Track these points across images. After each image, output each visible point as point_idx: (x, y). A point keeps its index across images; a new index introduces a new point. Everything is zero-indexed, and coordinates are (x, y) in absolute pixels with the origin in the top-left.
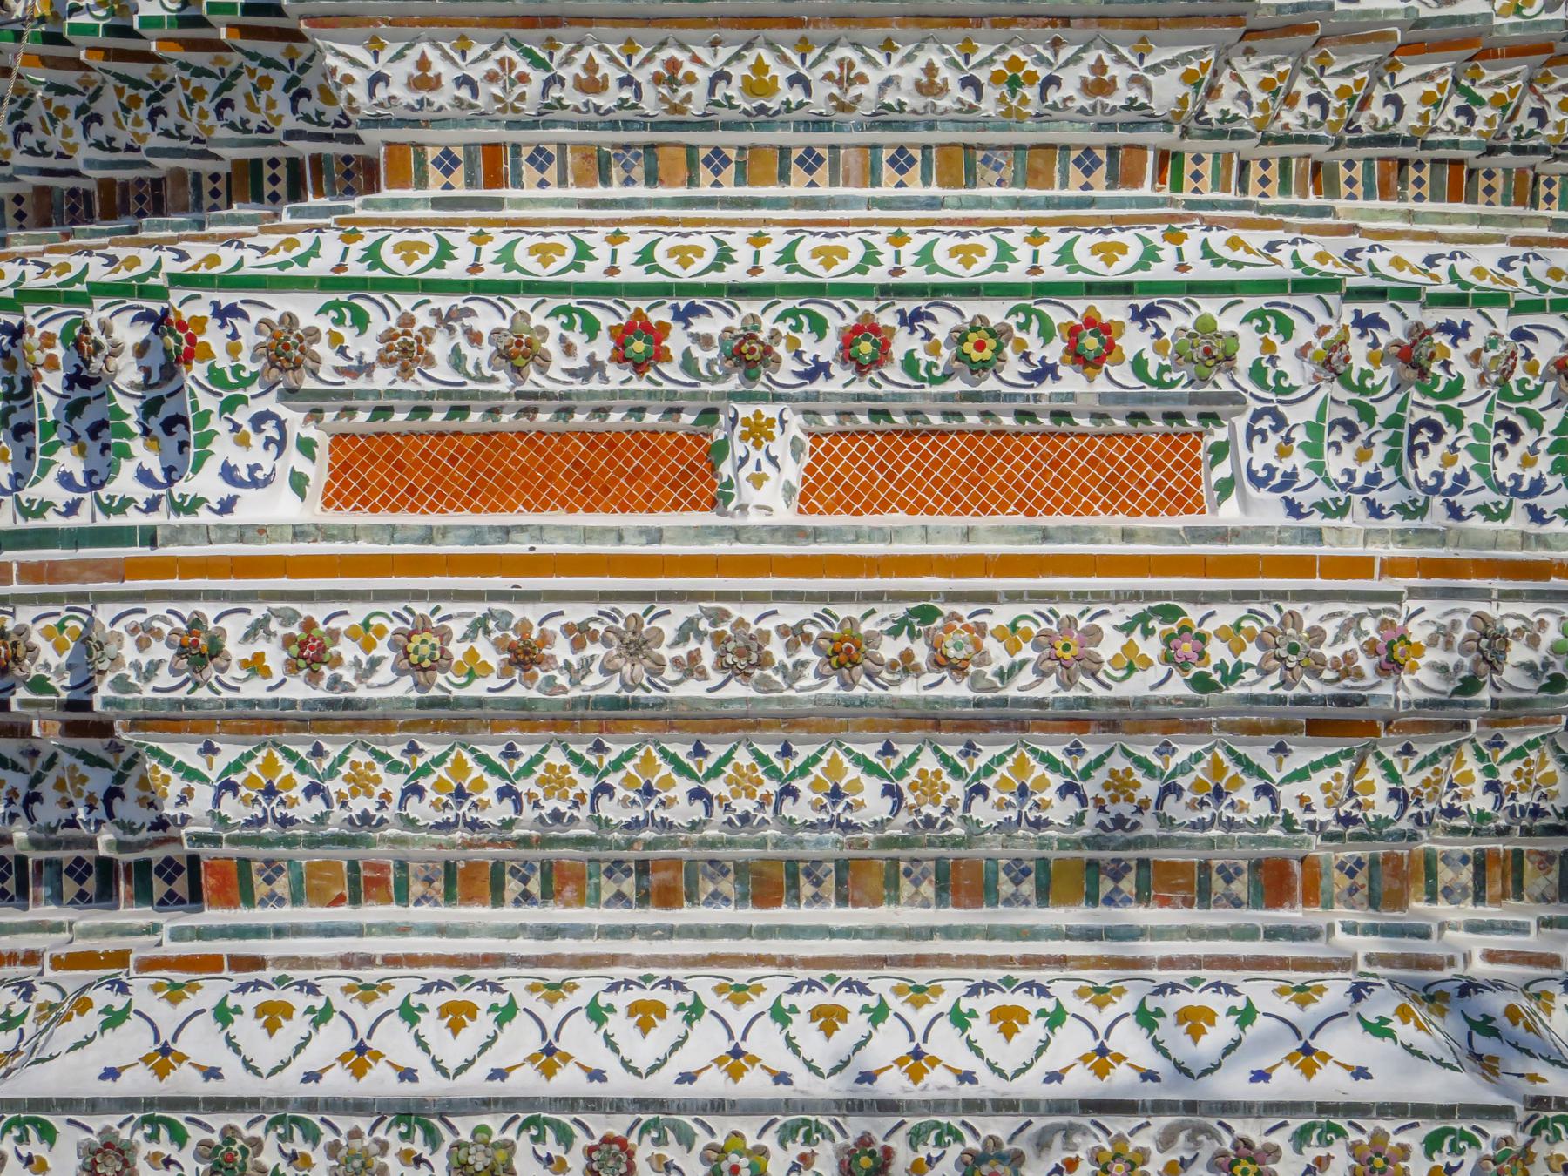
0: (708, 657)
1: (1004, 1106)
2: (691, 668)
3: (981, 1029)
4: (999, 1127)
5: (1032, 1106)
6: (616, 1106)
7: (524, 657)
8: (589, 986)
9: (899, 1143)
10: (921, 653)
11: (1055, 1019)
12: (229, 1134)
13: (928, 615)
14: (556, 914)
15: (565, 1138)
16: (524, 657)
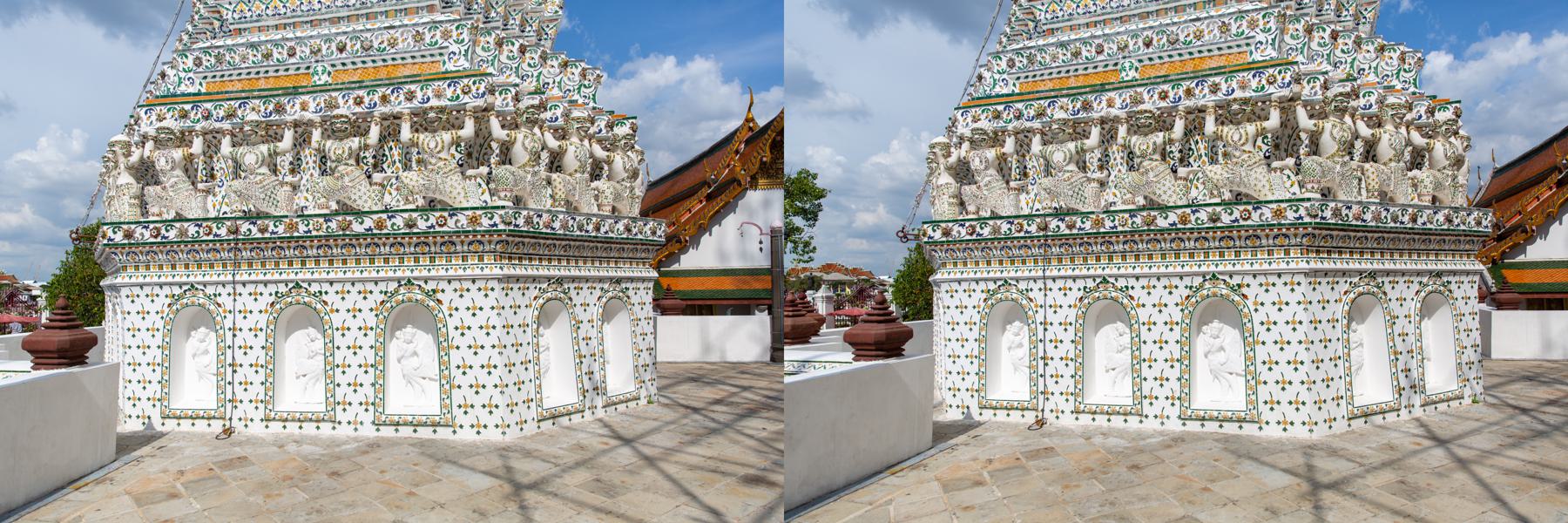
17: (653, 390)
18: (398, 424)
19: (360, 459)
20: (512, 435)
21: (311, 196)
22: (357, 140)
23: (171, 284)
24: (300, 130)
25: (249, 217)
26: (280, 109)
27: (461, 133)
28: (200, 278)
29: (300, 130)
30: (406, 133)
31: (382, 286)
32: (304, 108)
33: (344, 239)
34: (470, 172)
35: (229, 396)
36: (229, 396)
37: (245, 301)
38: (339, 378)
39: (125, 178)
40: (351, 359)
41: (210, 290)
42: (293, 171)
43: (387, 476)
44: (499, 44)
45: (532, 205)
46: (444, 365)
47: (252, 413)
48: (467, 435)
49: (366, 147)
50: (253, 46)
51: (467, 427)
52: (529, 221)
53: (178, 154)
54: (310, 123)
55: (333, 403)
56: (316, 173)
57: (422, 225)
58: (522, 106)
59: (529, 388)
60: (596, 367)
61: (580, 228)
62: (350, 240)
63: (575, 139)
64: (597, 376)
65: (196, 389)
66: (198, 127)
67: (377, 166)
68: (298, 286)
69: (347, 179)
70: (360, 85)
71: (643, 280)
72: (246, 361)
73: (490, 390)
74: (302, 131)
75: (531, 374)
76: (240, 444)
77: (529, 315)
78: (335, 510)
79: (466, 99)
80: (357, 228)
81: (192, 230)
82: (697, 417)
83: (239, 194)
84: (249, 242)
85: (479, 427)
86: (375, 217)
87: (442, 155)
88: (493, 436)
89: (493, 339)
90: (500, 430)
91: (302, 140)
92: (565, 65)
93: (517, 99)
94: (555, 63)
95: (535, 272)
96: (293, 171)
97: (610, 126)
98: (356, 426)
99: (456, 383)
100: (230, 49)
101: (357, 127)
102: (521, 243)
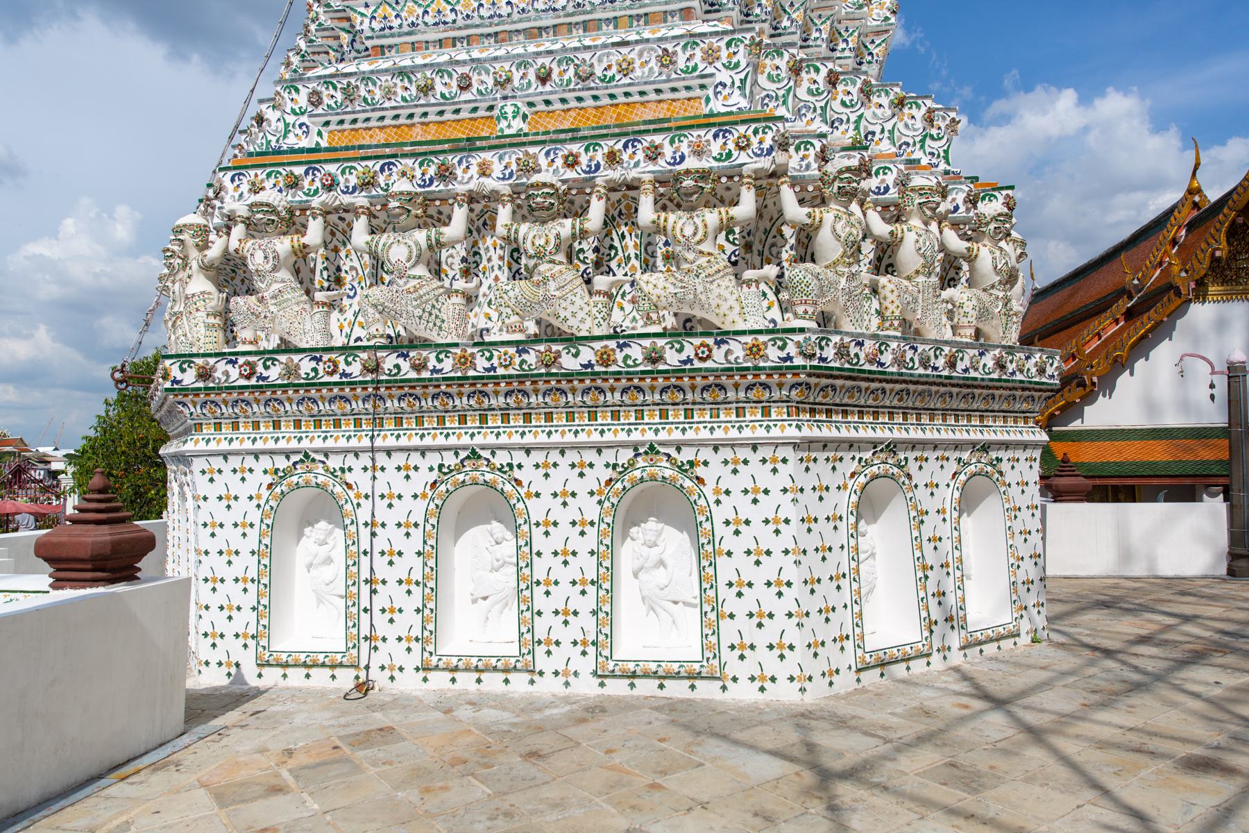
9: (554, 66)
12: (349, 84)
15: (450, 76)
17: (1041, 621)
18: (634, 675)
19: (573, 732)
20: (817, 693)
21: (496, 312)
22: (568, 222)
23: (271, 453)
24: (478, 207)
25: (396, 345)
26: (445, 174)
27: (735, 211)
28: (318, 443)
29: (478, 207)
30: (647, 212)
31: (609, 456)
32: (484, 171)
33: (548, 380)
34: (749, 274)
35: (365, 631)
36: (365, 631)
37: (391, 479)
38: (540, 602)
39: (200, 284)
40: (559, 572)
41: (335, 462)
42: (466, 273)
43: (617, 759)
44: (796, 70)
45: (847, 326)
46: (707, 581)
47: (401, 657)
48: (744, 693)
49: (584, 234)
50: (403, 73)
51: (744, 680)
52: (842, 351)
53: (283, 245)
54: (494, 196)
55: (530, 641)
56: (504, 276)
57: (672, 358)
58: (831, 168)
59: (844, 618)
60: (949, 585)
61: (925, 363)
62: (558, 383)
63: (915, 222)
64: (951, 599)
65: (312, 620)
66: (316, 202)
67: (601, 265)
68: (474, 455)
69: (552, 285)
70: (574, 135)
71: (1025, 446)
72: (392, 575)
73: (780, 621)
74: (482, 208)
75: (846, 596)
76: (382, 707)
77: (843, 502)
78: (534, 812)
79: (743, 158)
80: (570, 363)
81: (306, 366)
82: (1110, 664)
83: (381, 310)
84: (396, 386)
85: (762, 680)
86: (598, 345)
87: (705, 247)
88: (785, 694)
89: (786, 541)
90: (796, 685)
91: (481, 224)
92: (900, 103)
93: (823, 157)
94: (885, 101)
95: (853, 434)
96: (466, 273)
97: (972, 201)
98: (567, 678)
99: (727, 610)
100: (366, 78)
101: (569, 203)
102: (831, 387)
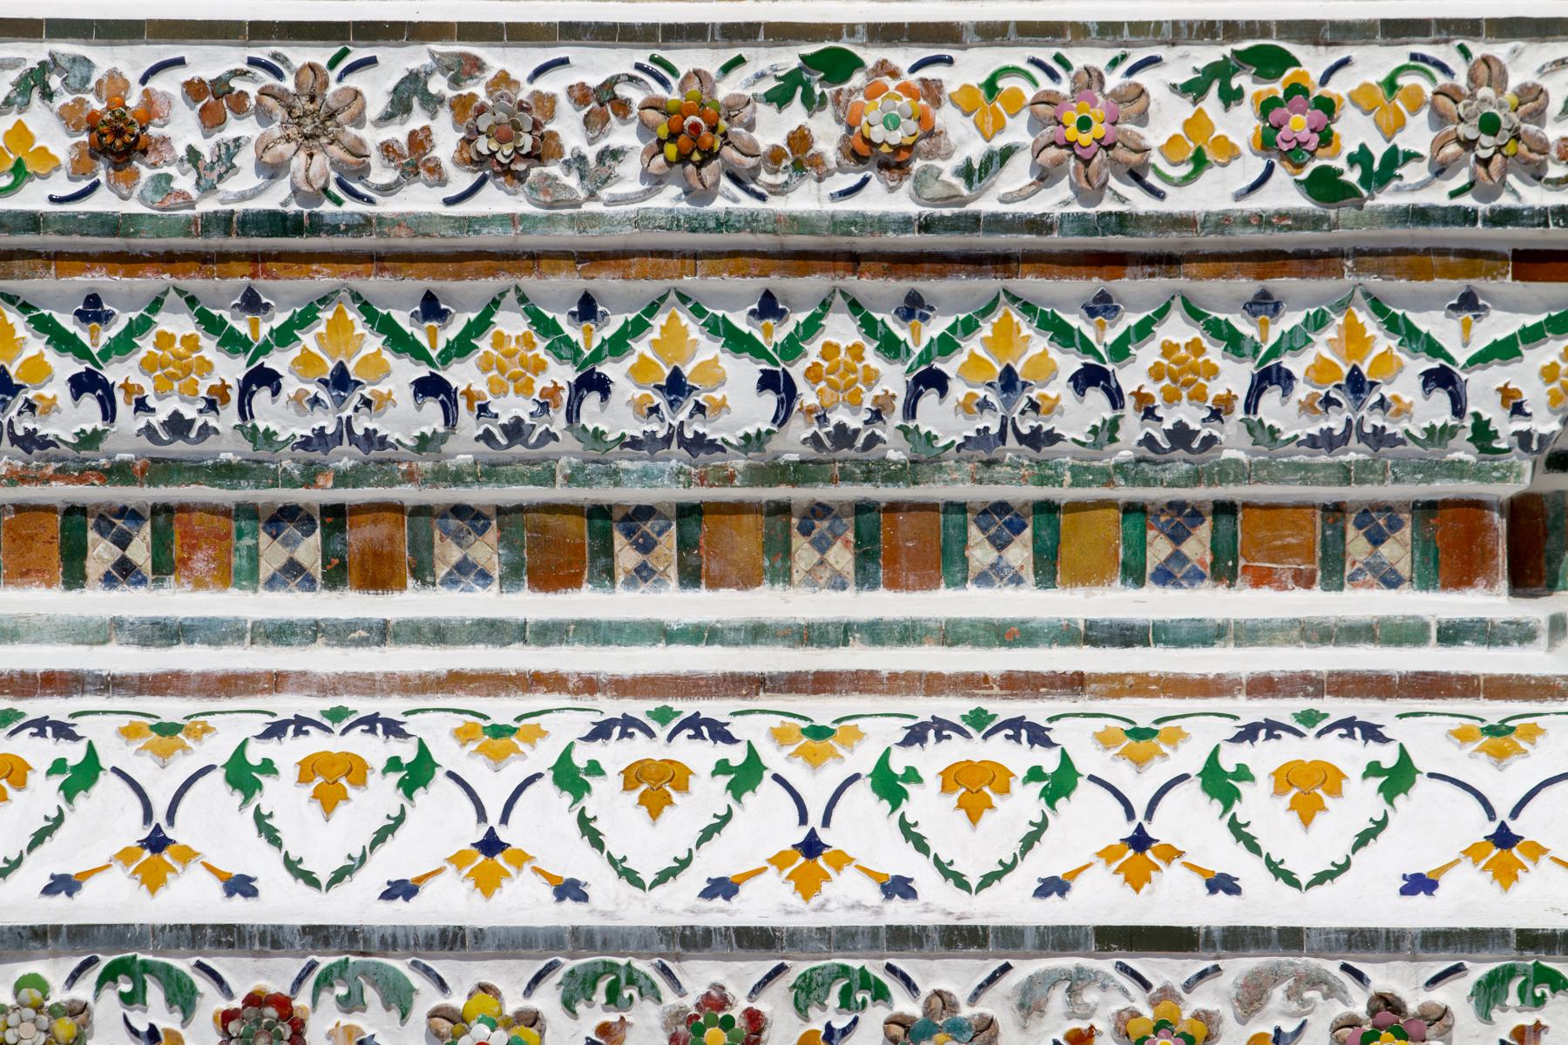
0: (446, 141)
1: (962, 938)
2: (415, 160)
3: (928, 806)
4: (954, 976)
5: (1010, 939)
6: (271, 940)
7: (117, 142)
8: (232, 727)
10: (827, 135)
11: (1059, 785)
13: (838, 66)
14: (175, 601)
16: (117, 142)
